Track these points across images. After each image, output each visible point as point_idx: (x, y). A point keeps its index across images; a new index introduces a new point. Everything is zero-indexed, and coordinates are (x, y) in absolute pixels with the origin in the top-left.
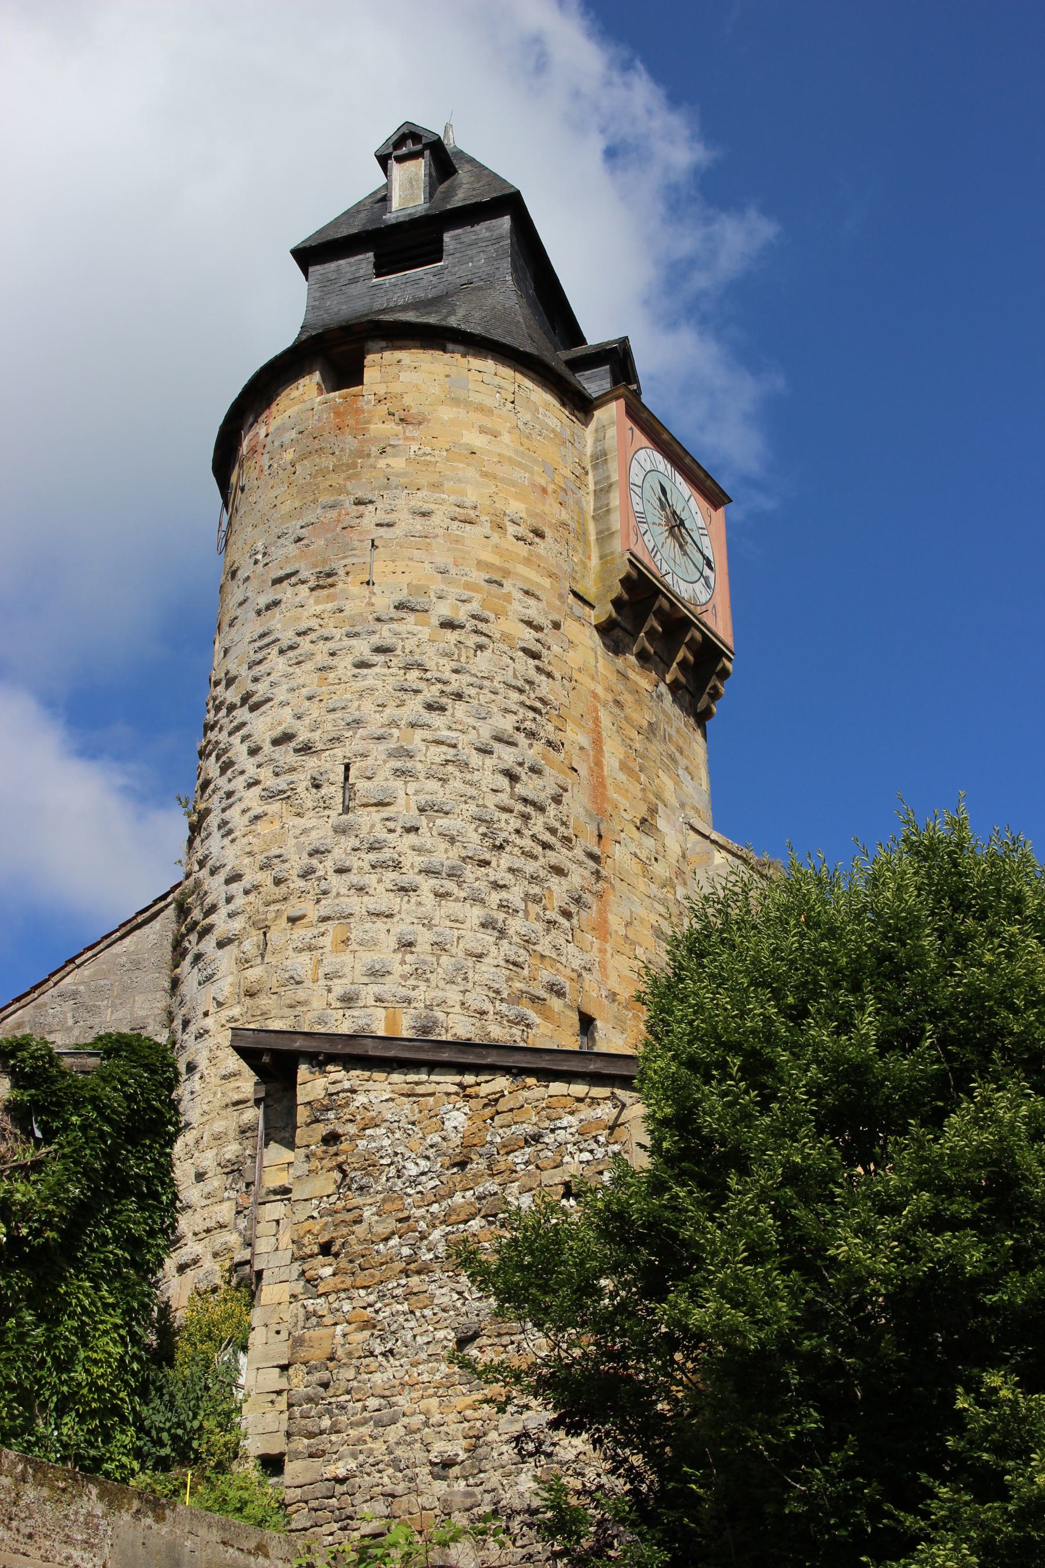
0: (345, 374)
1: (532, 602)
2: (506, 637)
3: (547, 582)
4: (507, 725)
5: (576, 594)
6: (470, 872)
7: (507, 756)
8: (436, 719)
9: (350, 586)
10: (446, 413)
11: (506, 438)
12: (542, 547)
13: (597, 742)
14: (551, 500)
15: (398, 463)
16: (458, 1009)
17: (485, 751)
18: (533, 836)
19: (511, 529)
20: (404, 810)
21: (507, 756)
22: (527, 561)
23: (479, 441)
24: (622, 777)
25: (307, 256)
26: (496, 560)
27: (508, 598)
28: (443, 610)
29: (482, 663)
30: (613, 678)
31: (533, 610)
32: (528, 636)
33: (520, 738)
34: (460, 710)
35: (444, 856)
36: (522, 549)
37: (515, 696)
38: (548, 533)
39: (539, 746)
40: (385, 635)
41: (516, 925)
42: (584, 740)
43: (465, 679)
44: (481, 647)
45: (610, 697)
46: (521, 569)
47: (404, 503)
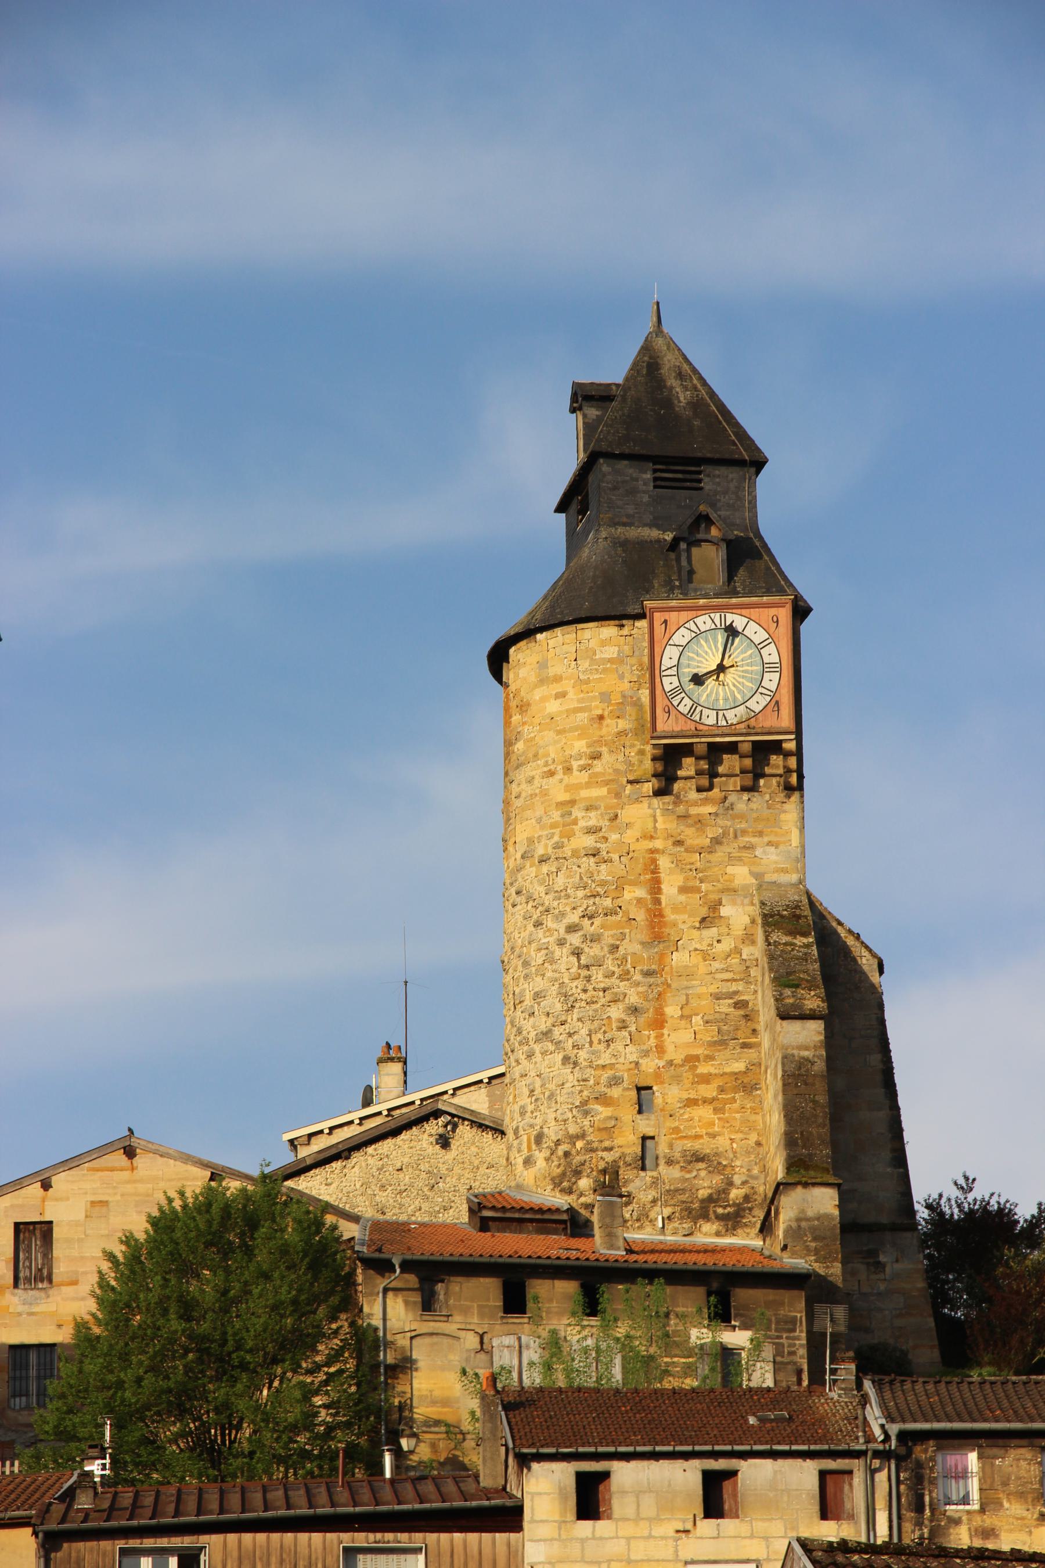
1: (592, 814)
2: (575, 853)
3: (603, 791)
4: (574, 918)
5: (630, 782)
8: (540, 933)
11: (571, 695)
12: (598, 766)
14: (607, 721)
16: (553, 1123)
17: (561, 943)
18: (594, 989)
19: (575, 765)
22: (588, 785)
23: (553, 707)
24: (682, 898)
26: (566, 797)
27: (575, 822)
28: (540, 851)
29: (560, 881)
31: (593, 819)
32: (589, 841)
33: (586, 922)
36: (584, 777)
37: (580, 893)
38: (604, 750)
39: (597, 921)
41: (583, 1055)
42: (641, 892)
43: (551, 896)
44: (559, 870)
45: (670, 842)
46: (584, 793)
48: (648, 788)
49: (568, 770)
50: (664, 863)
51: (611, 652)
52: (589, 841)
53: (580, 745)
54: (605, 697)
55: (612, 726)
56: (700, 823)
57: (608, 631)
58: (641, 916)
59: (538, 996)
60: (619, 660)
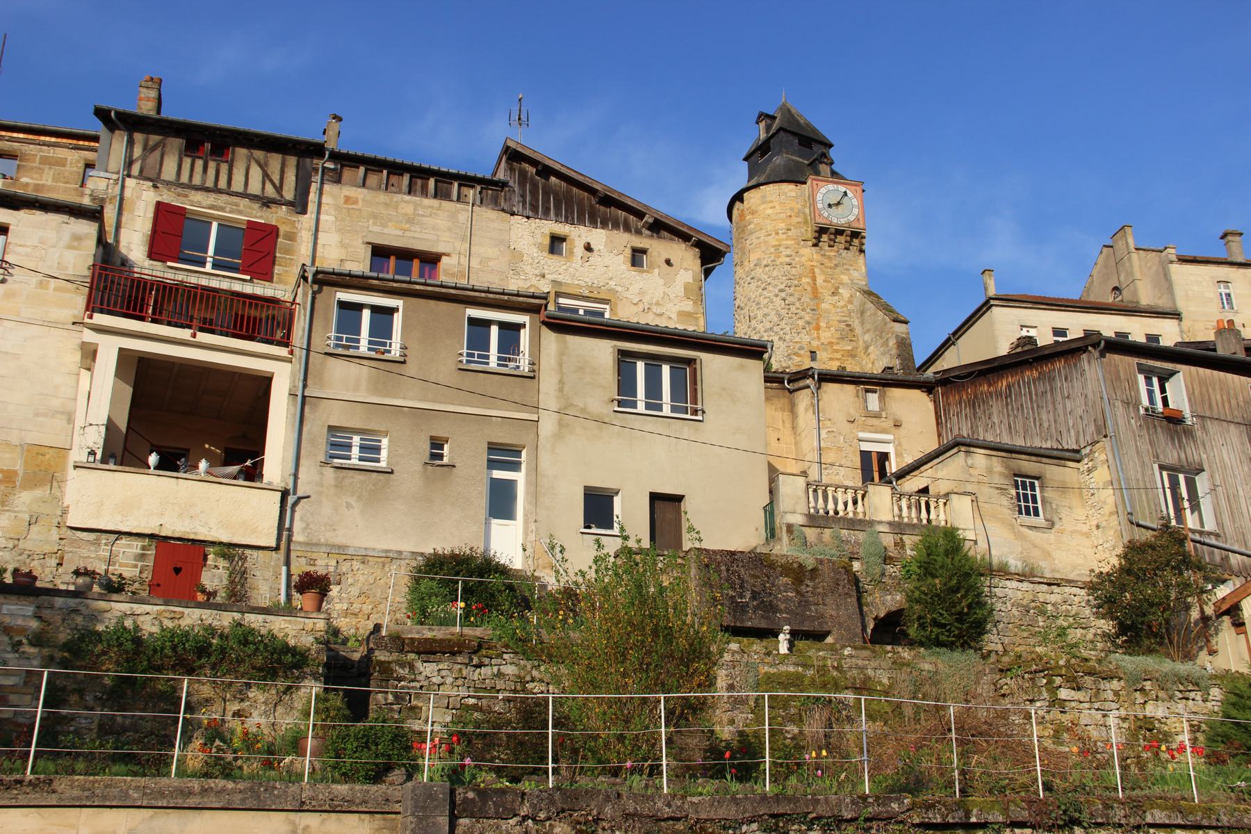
0: (742, 201)
2: (781, 264)
4: (782, 287)
6: (775, 328)
7: (783, 295)
9: (746, 263)
10: (761, 207)
12: (790, 233)
13: (814, 279)
15: (752, 226)
20: (759, 317)
21: (783, 295)
23: (769, 211)
25: (745, 159)
29: (775, 273)
30: (820, 257)
31: (788, 252)
32: (788, 260)
34: (770, 288)
35: (768, 326)
40: (753, 274)
42: (809, 280)
47: (753, 237)
48: (810, 243)
49: (777, 234)
50: (817, 270)
51: (793, 194)
52: (788, 260)
53: (782, 225)
54: (792, 209)
55: (795, 220)
56: (829, 258)
57: (791, 186)
58: (809, 289)
59: (765, 315)
60: (796, 197)
